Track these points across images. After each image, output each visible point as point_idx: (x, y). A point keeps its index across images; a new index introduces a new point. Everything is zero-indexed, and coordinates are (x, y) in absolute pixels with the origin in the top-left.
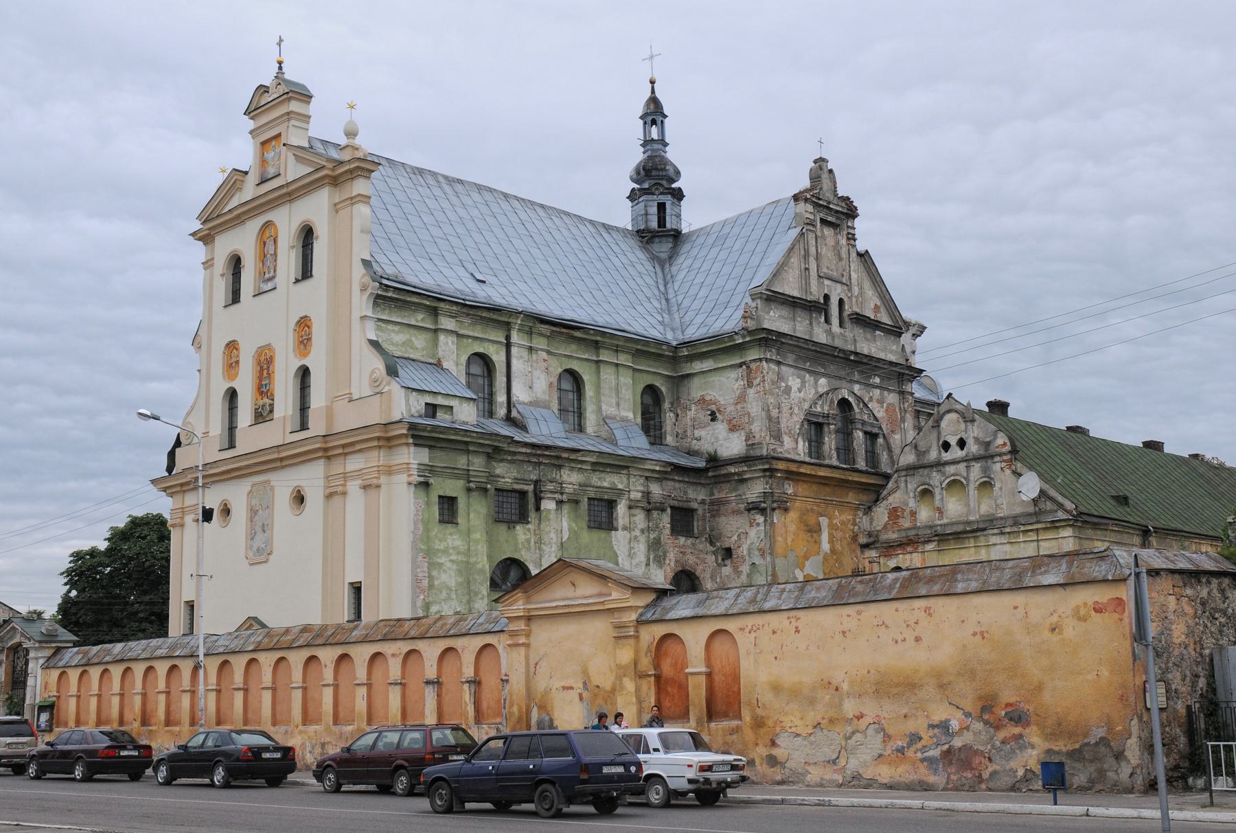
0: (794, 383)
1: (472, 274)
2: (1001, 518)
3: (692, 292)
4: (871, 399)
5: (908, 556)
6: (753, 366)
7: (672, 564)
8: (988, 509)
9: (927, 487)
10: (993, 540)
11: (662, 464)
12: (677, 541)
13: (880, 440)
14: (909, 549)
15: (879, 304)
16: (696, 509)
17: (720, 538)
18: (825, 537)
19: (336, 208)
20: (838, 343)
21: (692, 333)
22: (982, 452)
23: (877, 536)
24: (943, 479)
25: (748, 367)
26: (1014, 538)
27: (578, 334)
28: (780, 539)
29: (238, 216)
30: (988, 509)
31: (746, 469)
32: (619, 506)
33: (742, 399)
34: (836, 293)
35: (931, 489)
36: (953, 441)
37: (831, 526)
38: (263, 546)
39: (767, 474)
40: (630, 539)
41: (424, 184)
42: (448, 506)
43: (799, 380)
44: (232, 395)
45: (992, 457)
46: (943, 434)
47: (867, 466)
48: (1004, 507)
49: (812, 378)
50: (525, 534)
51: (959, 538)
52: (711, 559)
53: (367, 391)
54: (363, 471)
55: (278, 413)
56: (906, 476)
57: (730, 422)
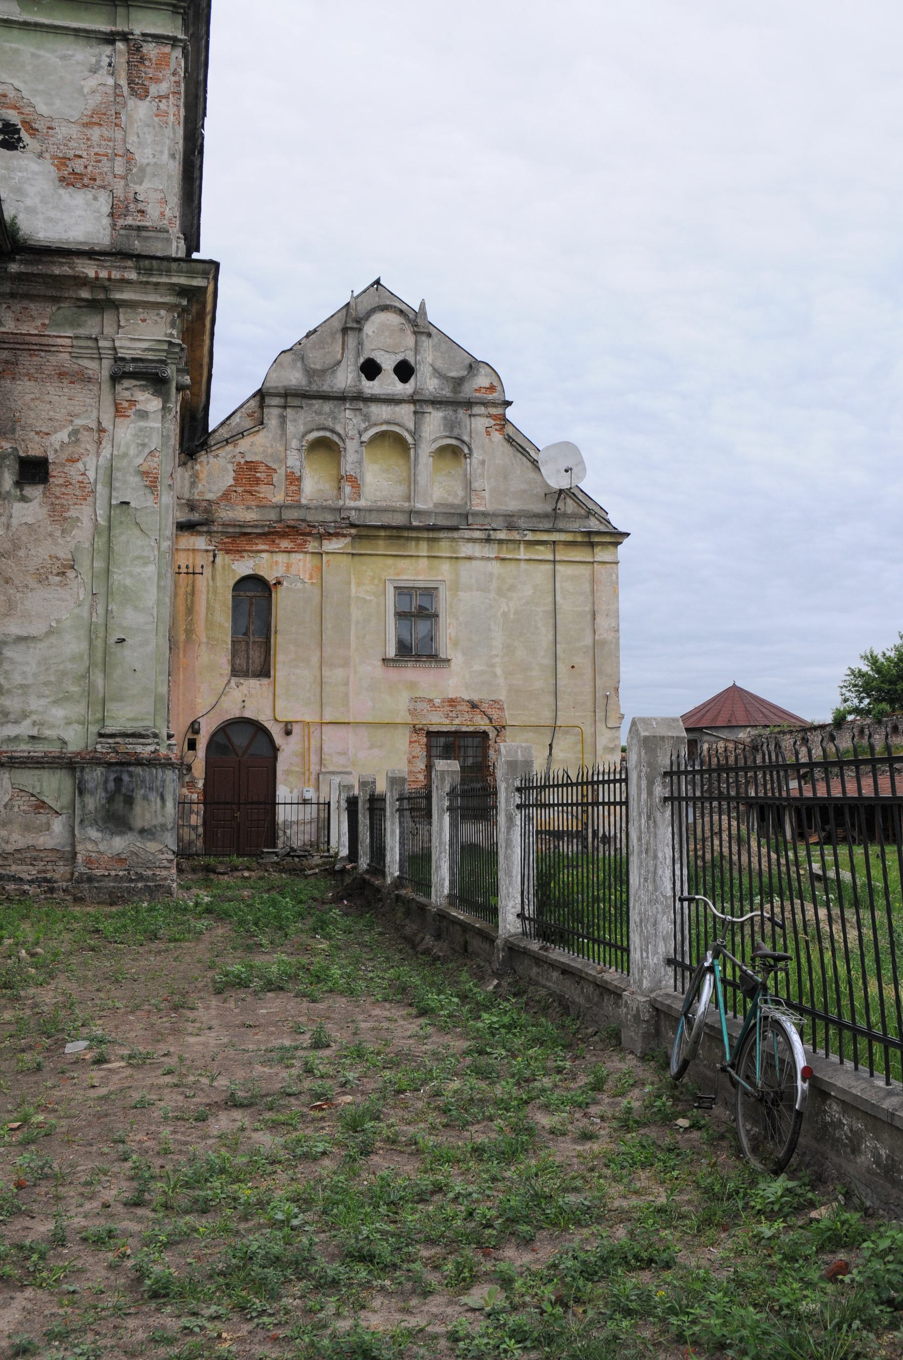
2: (484, 514)
5: (281, 558)
6: (151, 50)
8: (446, 495)
10: (467, 549)
14: (285, 544)
17: (13, 431)
22: (447, 393)
24: (363, 426)
25: (135, 49)
26: (508, 551)
30: (446, 495)
31: (133, 276)
35: (335, 438)
36: (388, 363)
45: (469, 404)
46: (368, 345)
48: (486, 494)
51: (399, 537)
56: (285, 407)
57: (62, 162)
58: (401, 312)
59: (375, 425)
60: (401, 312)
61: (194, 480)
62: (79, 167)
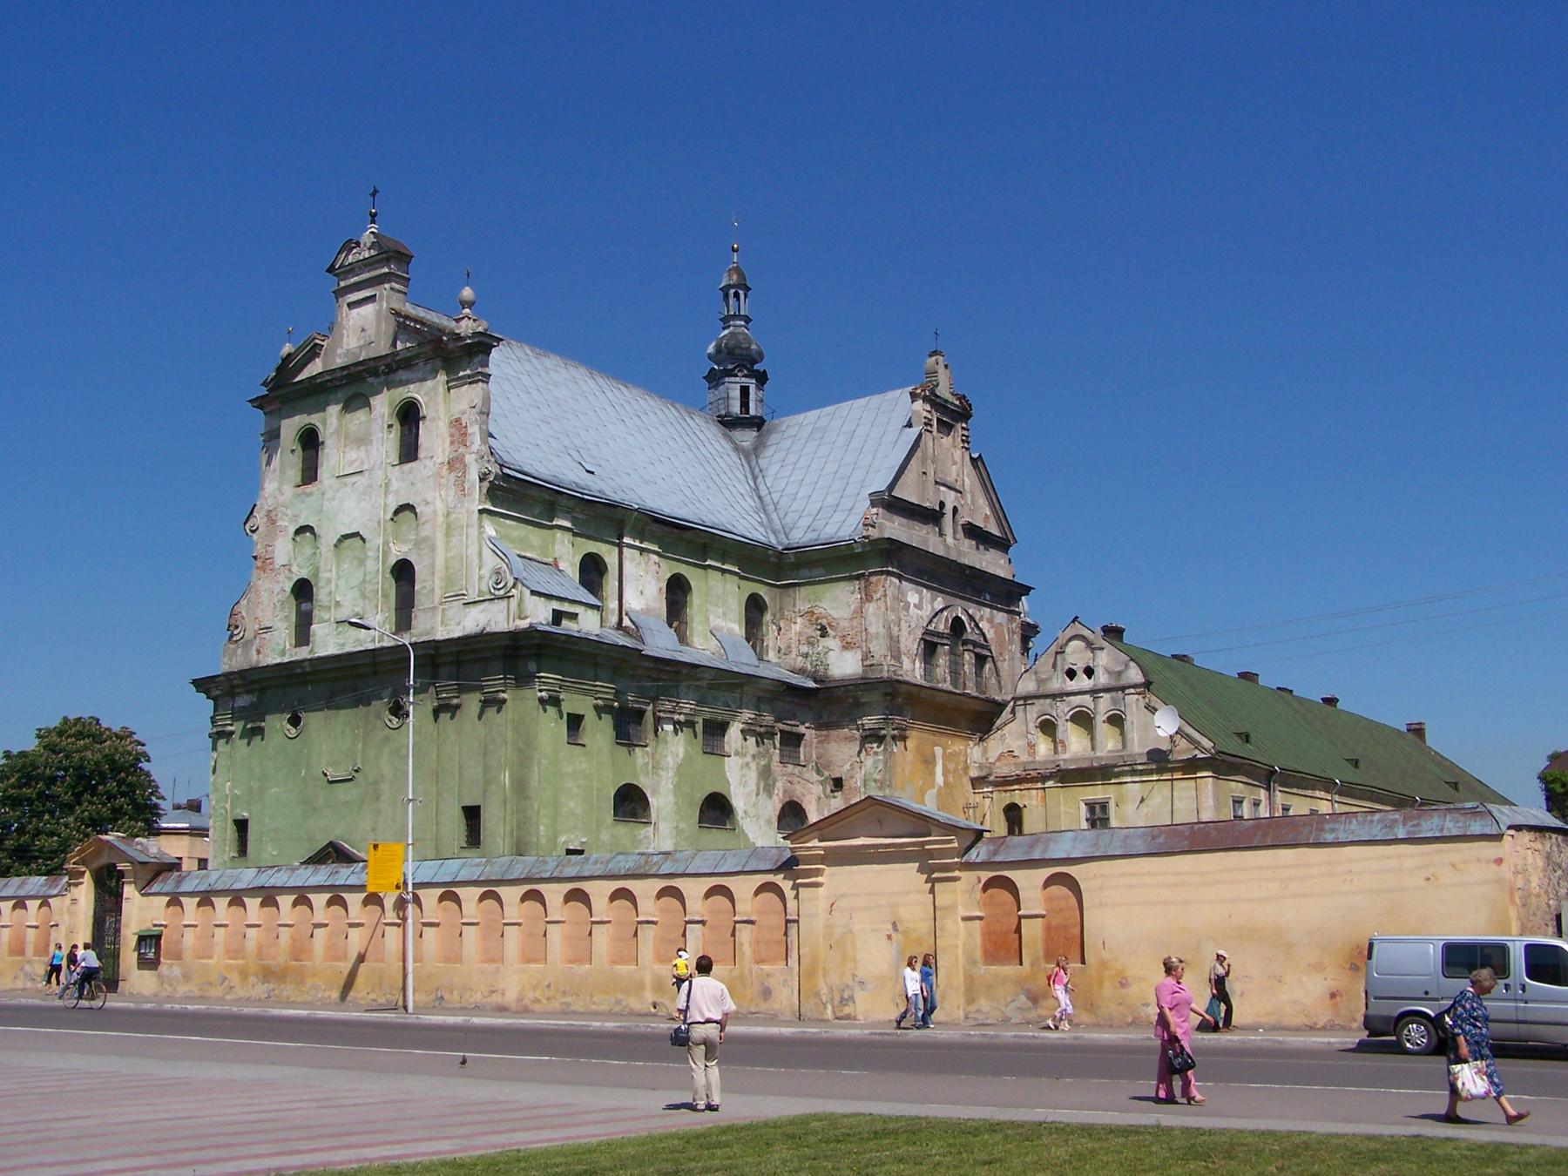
0: (913, 598)
1: (580, 463)
3: (791, 489)
4: (982, 618)
7: (781, 795)
9: (1048, 717)
11: (777, 683)
12: (785, 769)
13: (988, 666)
15: (988, 513)
16: (804, 735)
17: (829, 767)
18: (939, 769)
20: (953, 556)
21: (799, 536)
22: (1113, 683)
23: (990, 768)
27: (689, 535)
28: (899, 770)
32: (732, 729)
33: (860, 612)
34: (950, 499)
36: (1079, 668)
37: (945, 757)
39: (889, 698)
40: (742, 765)
41: (515, 358)
42: (575, 722)
43: (917, 596)
47: (977, 691)
49: (929, 594)
50: (644, 757)
52: (817, 789)
61: (985, 751)
62: (850, 641)
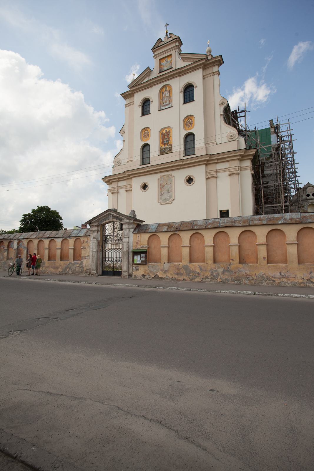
19: (204, 77)
29: (150, 84)
38: (169, 198)
44: (145, 148)
53: (225, 140)
54: (229, 169)
55: (174, 149)
58: (312, 186)
59: (309, 203)
60: (312, 186)
